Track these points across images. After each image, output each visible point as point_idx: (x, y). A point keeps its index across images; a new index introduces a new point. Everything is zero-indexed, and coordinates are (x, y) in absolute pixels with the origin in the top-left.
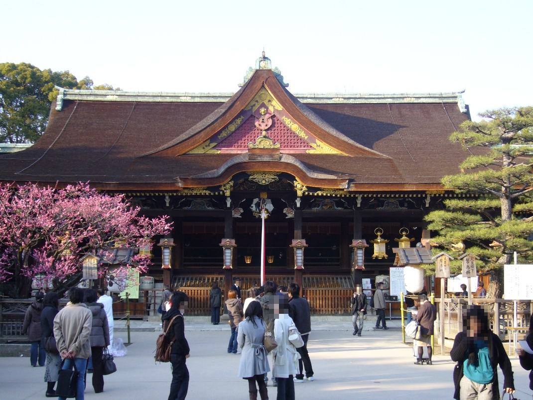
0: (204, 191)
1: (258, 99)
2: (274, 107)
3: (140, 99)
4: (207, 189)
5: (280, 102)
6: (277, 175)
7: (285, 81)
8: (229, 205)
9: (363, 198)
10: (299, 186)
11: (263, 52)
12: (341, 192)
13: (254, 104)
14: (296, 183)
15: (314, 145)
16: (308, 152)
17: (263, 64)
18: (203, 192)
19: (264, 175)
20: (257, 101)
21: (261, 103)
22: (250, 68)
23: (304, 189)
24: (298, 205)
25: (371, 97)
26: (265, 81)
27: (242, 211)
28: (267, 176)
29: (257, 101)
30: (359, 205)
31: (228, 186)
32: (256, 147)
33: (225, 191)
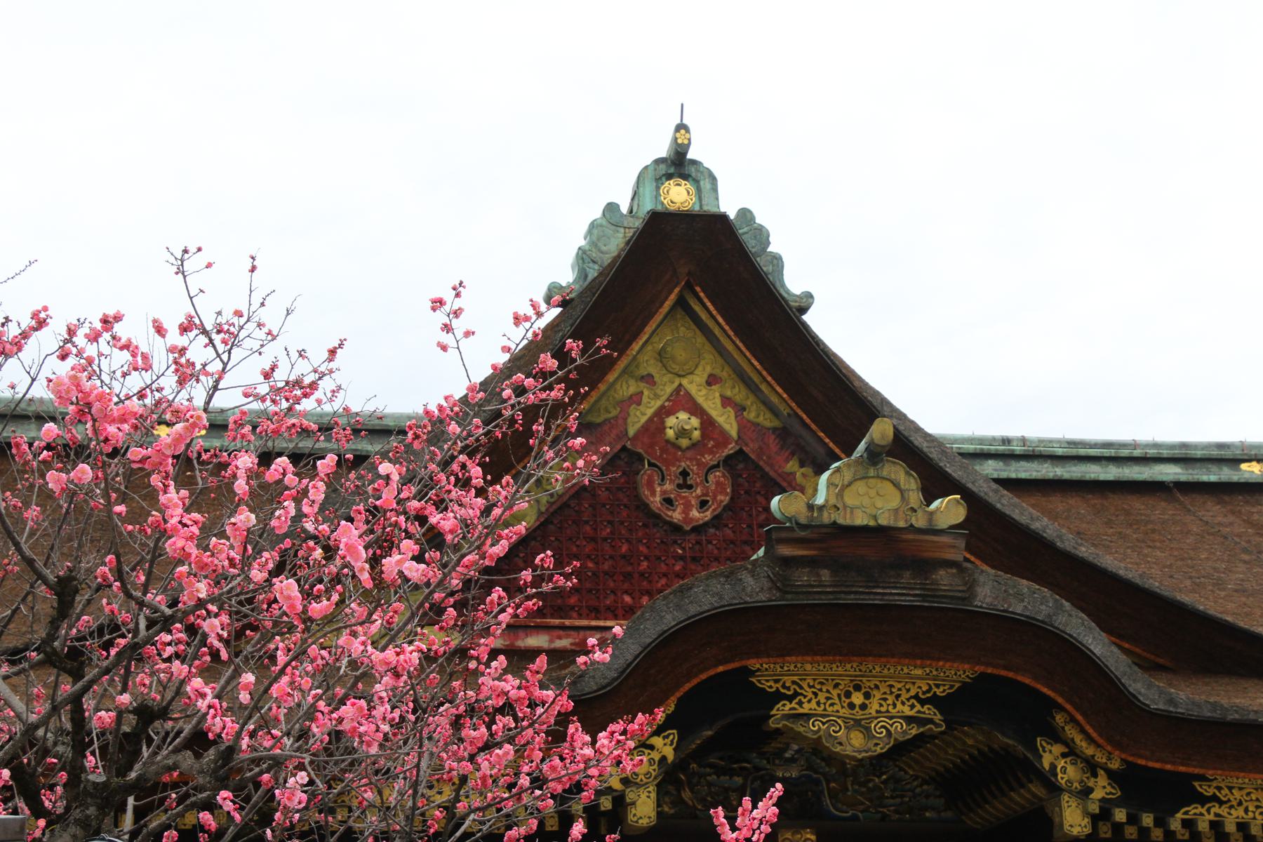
1: (652, 368)
2: (740, 409)
6: (934, 701)
7: (794, 282)
10: (1068, 773)
11: (681, 127)
13: (632, 390)
14: (1050, 755)
17: (678, 195)
19: (857, 698)
20: (649, 379)
21: (669, 389)
22: (611, 208)
23: (1102, 789)
25: (1082, 452)
26: (682, 270)
29: (649, 379)
33: (630, 796)
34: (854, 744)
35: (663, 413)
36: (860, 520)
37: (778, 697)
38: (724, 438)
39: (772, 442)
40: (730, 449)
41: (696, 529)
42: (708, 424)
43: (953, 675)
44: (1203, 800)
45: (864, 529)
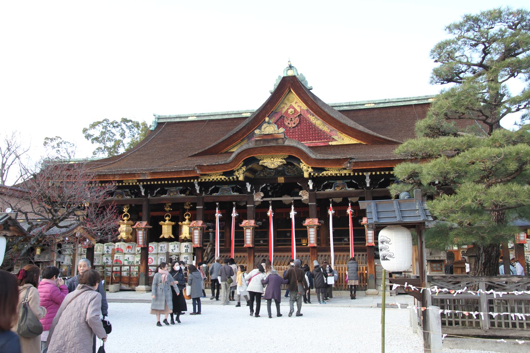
0: (221, 177)
3: (212, 118)
4: (224, 174)
5: (304, 103)
6: (284, 159)
7: (309, 85)
8: (249, 190)
9: (371, 176)
12: (345, 171)
15: (335, 137)
16: (330, 143)
17: (290, 73)
18: (219, 178)
19: (272, 159)
22: (279, 76)
23: (310, 170)
24: (311, 187)
26: (290, 85)
27: (262, 195)
28: (275, 160)
29: (286, 104)
30: (368, 185)
31: (241, 171)
32: (262, 133)
34: (272, 166)
35: (288, 109)
36: (267, 133)
37: (260, 160)
38: (298, 112)
39: (306, 112)
40: (299, 114)
41: (293, 128)
42: (295, 110)
43: (286, 155)
44: (326, 171)
45: (268, 134)
